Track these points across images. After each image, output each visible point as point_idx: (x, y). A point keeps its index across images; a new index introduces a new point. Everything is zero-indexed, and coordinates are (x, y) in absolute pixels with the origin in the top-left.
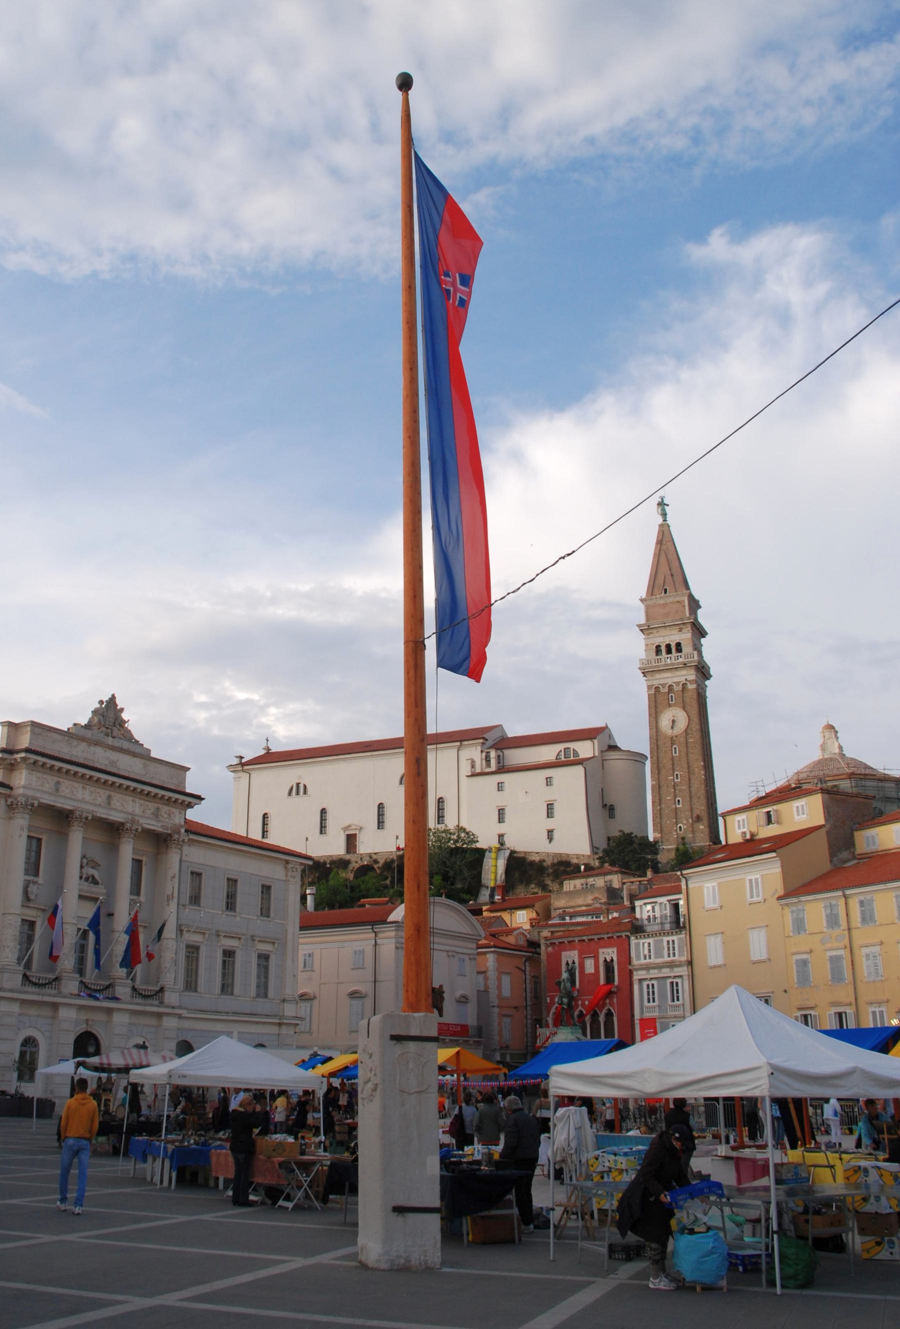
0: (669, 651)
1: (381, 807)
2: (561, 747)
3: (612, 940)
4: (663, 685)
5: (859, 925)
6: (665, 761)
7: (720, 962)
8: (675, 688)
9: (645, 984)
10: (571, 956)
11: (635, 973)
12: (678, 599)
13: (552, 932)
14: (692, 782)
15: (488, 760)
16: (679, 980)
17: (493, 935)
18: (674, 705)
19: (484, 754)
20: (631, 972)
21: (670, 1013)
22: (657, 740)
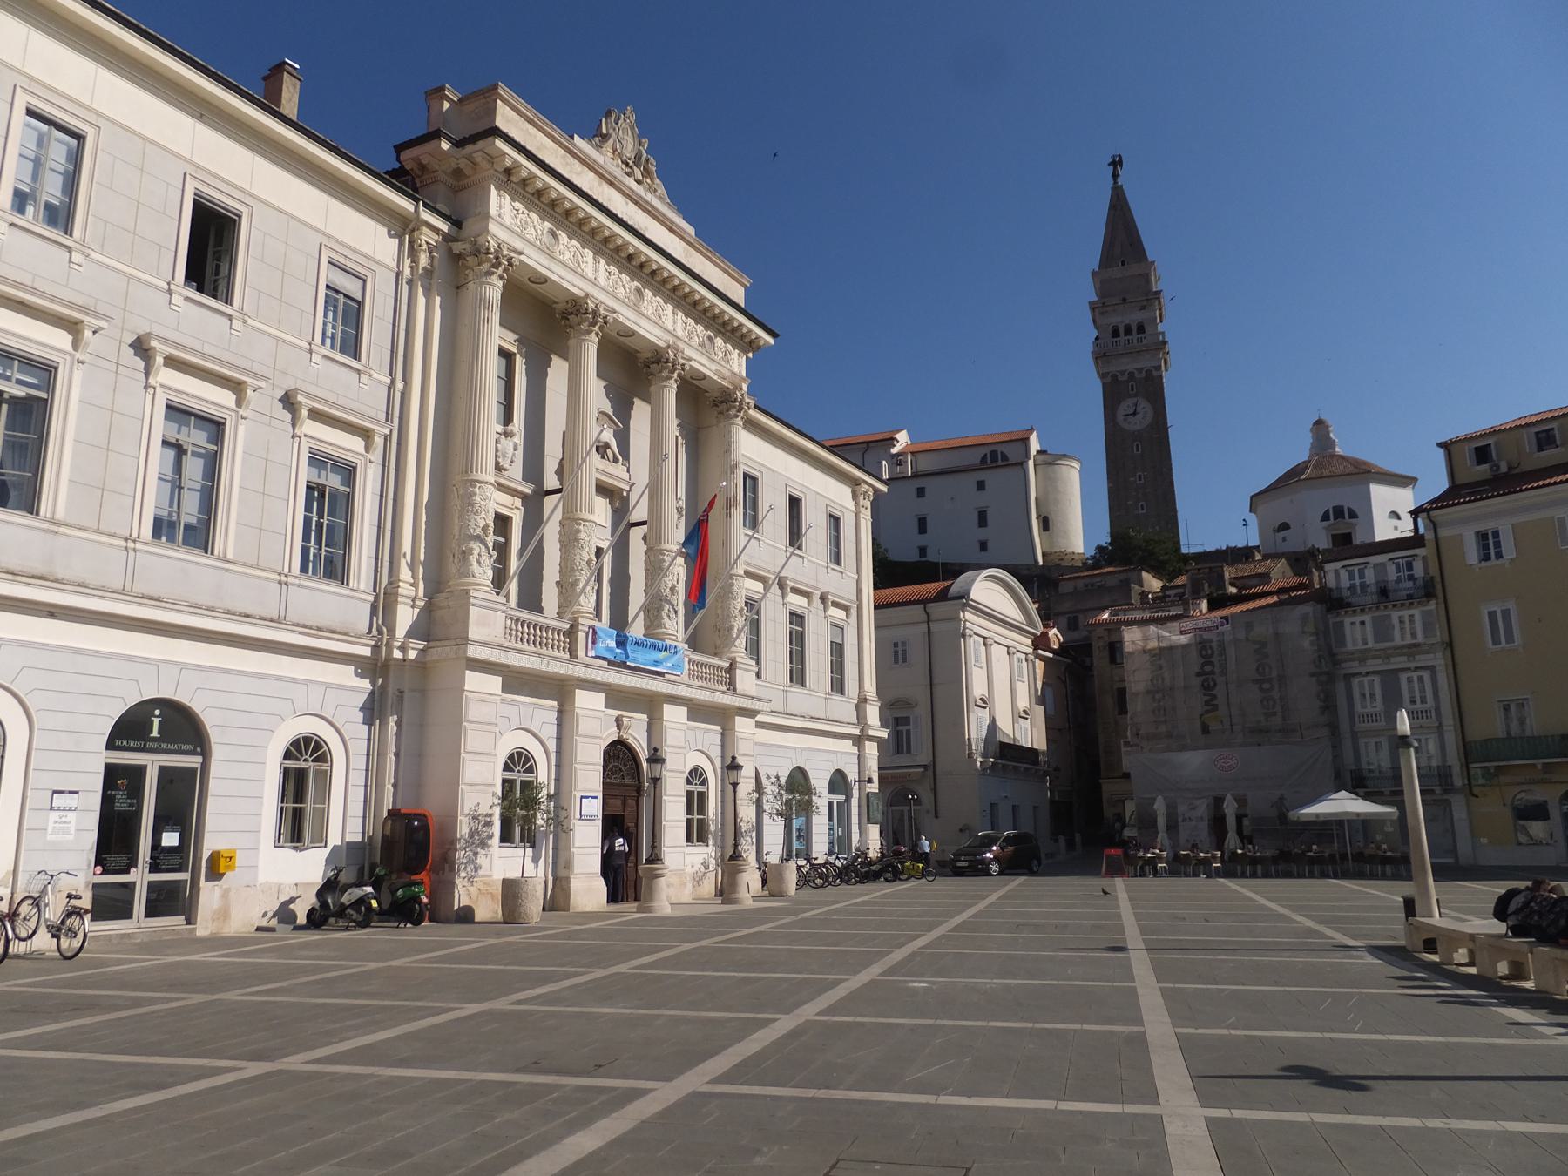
4: (1123, 373)
8: (1137, 376)
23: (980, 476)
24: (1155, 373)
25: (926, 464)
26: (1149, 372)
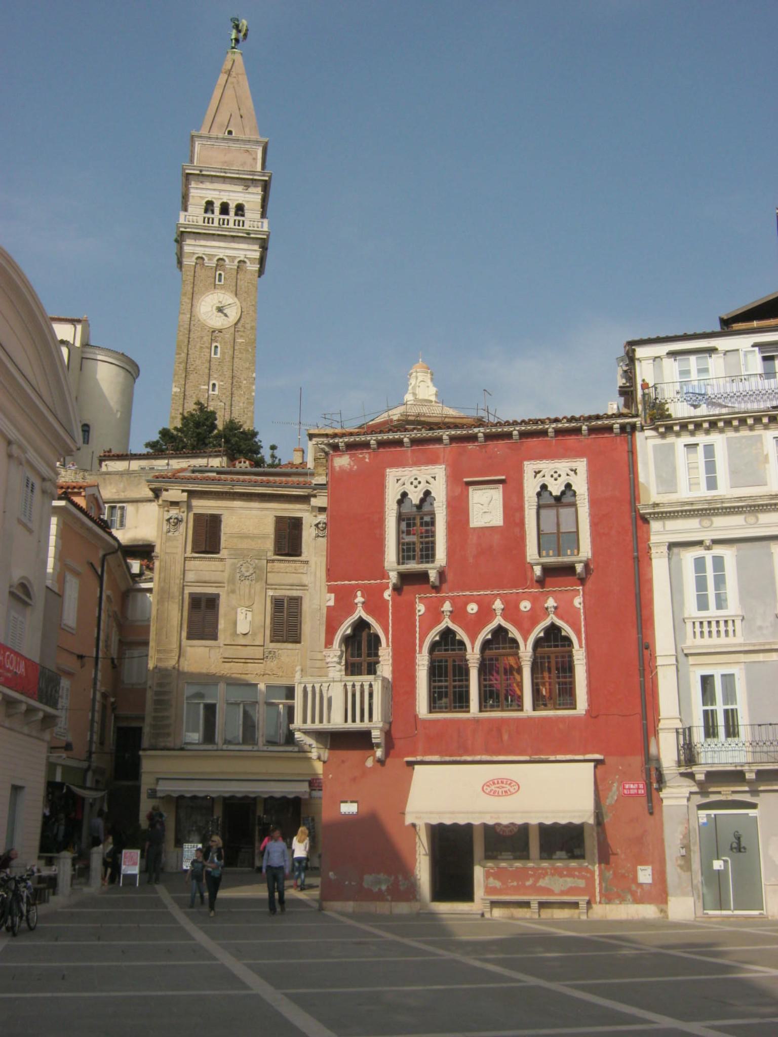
3: (571, 440)
4: (211, 256)
6: (198, 362)
9: (688, 557)
11: (655, 526)
13: (192, 494)
14: (236, 398)
22: (190, 331)
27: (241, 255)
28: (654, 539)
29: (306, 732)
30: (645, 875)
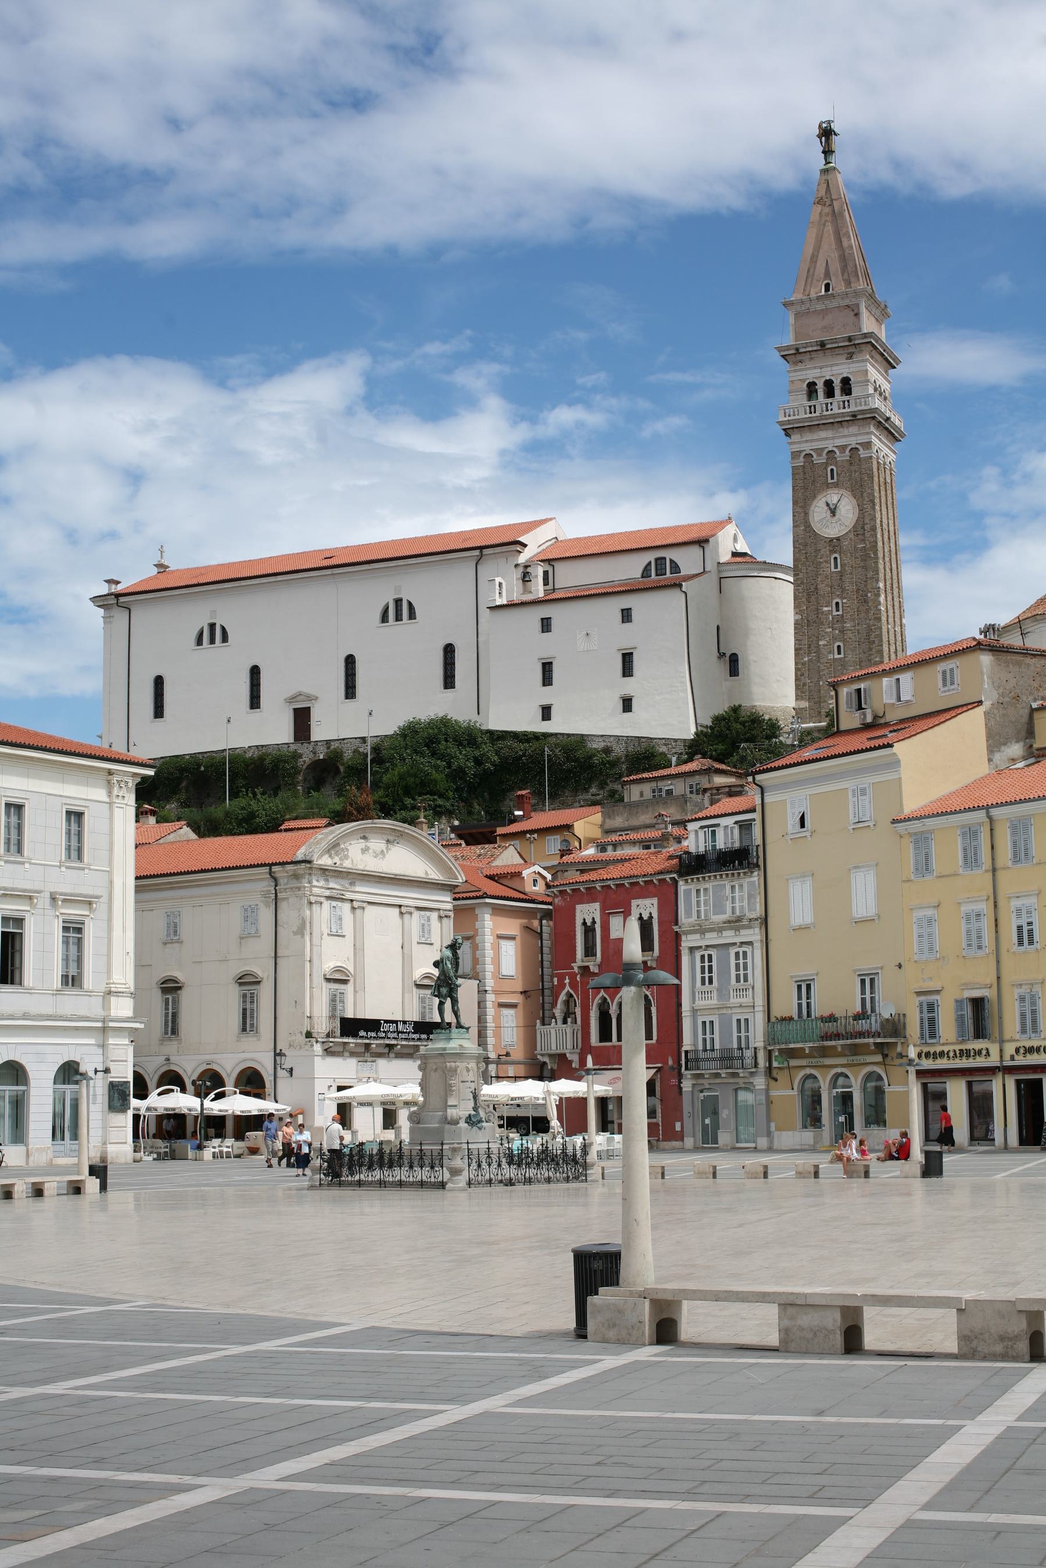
0: (830, 393)
1: (350, 661)
2: (651, 557)
3: (651, 888)
5: (1010, 864)
7: (808, 919)
9: (698, 955)
10: (588, 912)
11: (684, 938)
12: (847, 302)
15: (526, 578)
16: (747, 949)
17: (491, 877)
18: (836, 485)
19: (521, 569)
20: (678, 937)
21: (734, 1001)
23: (625, 602)
24: (863, 453)
25: (568, 577)
26: (854, 450)
27: (853, 441)
28: (683, 944)
29: (542, 1055)
30: (678, 1127)
